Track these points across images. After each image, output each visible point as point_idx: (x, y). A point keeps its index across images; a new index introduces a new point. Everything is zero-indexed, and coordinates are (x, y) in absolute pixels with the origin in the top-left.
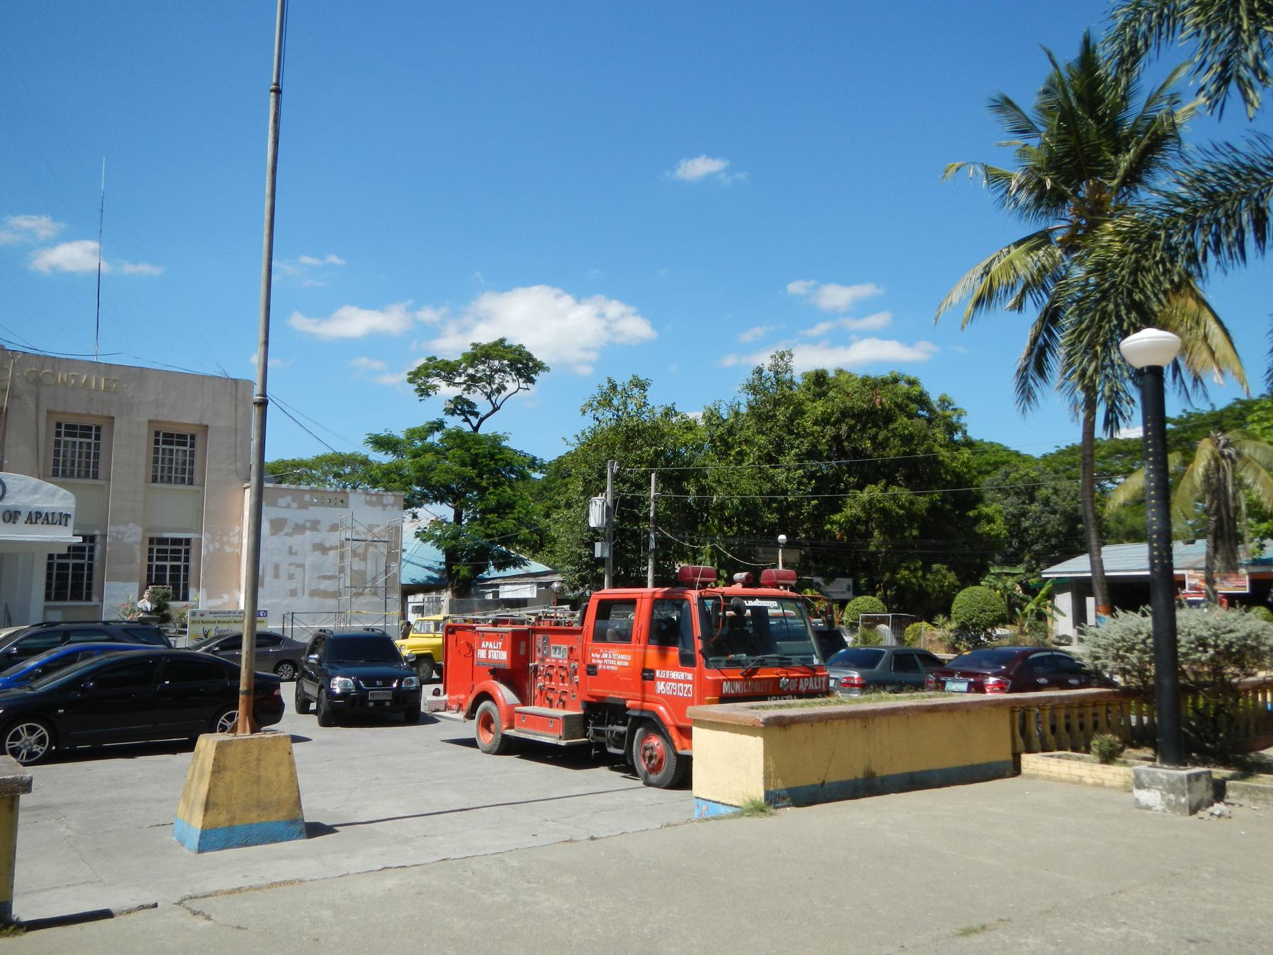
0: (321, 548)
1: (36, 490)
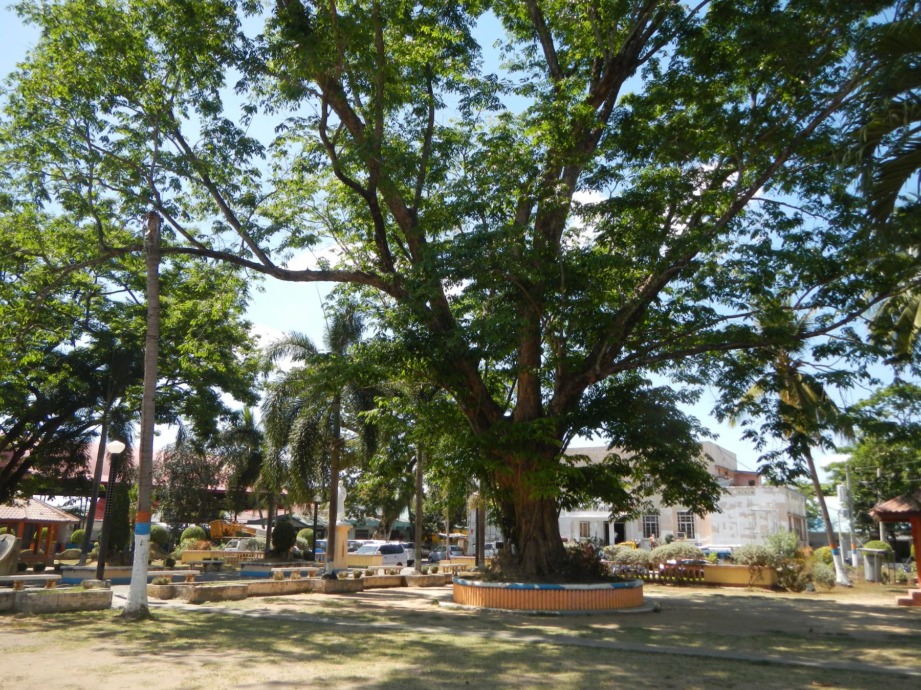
0: (743, 515)
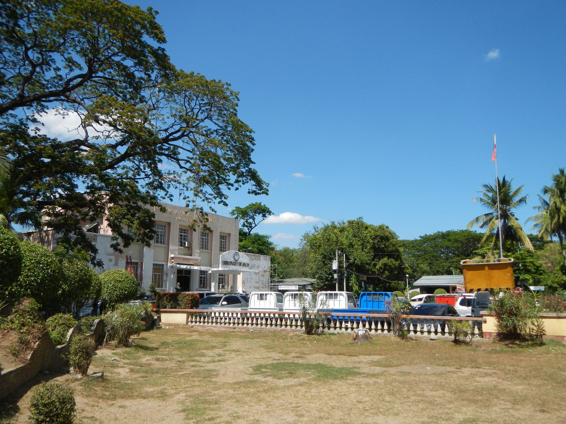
1: (243, 257)
